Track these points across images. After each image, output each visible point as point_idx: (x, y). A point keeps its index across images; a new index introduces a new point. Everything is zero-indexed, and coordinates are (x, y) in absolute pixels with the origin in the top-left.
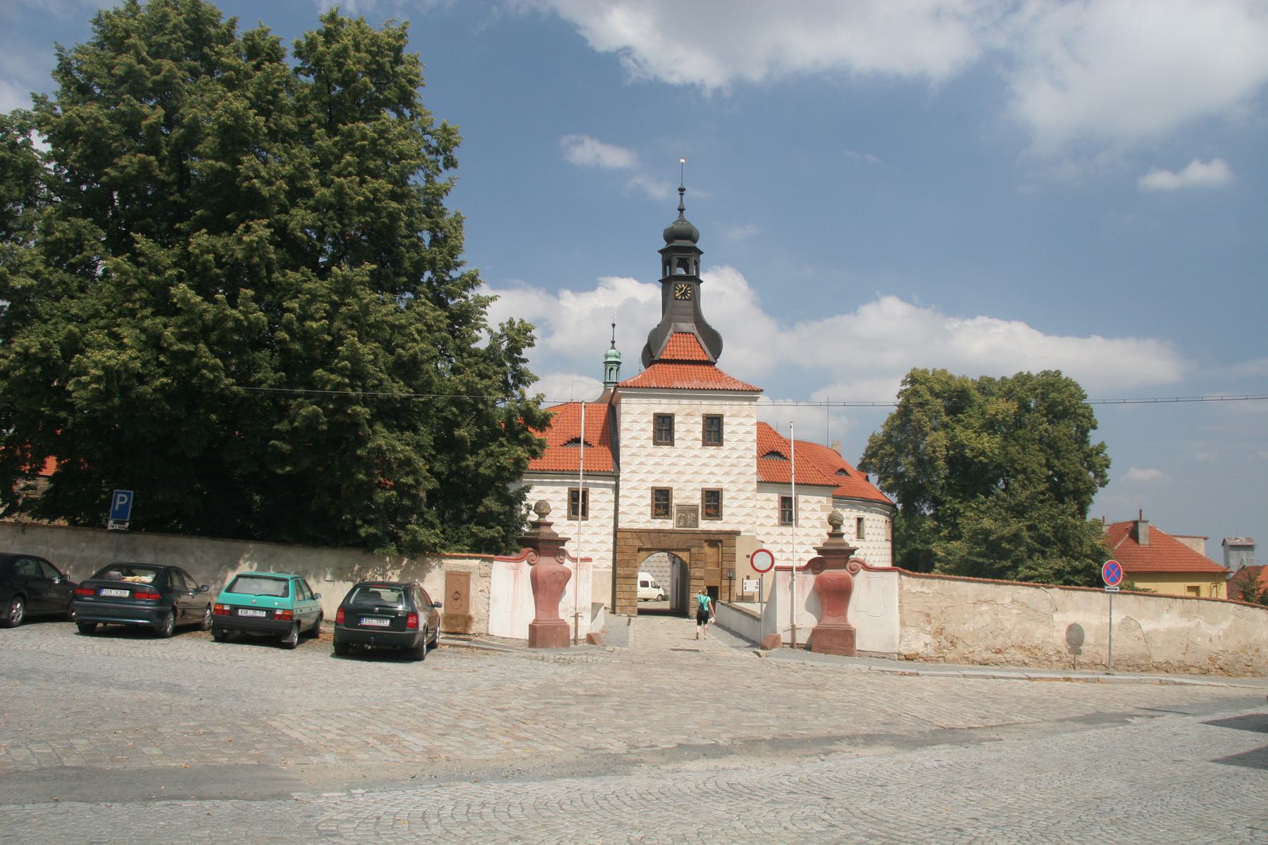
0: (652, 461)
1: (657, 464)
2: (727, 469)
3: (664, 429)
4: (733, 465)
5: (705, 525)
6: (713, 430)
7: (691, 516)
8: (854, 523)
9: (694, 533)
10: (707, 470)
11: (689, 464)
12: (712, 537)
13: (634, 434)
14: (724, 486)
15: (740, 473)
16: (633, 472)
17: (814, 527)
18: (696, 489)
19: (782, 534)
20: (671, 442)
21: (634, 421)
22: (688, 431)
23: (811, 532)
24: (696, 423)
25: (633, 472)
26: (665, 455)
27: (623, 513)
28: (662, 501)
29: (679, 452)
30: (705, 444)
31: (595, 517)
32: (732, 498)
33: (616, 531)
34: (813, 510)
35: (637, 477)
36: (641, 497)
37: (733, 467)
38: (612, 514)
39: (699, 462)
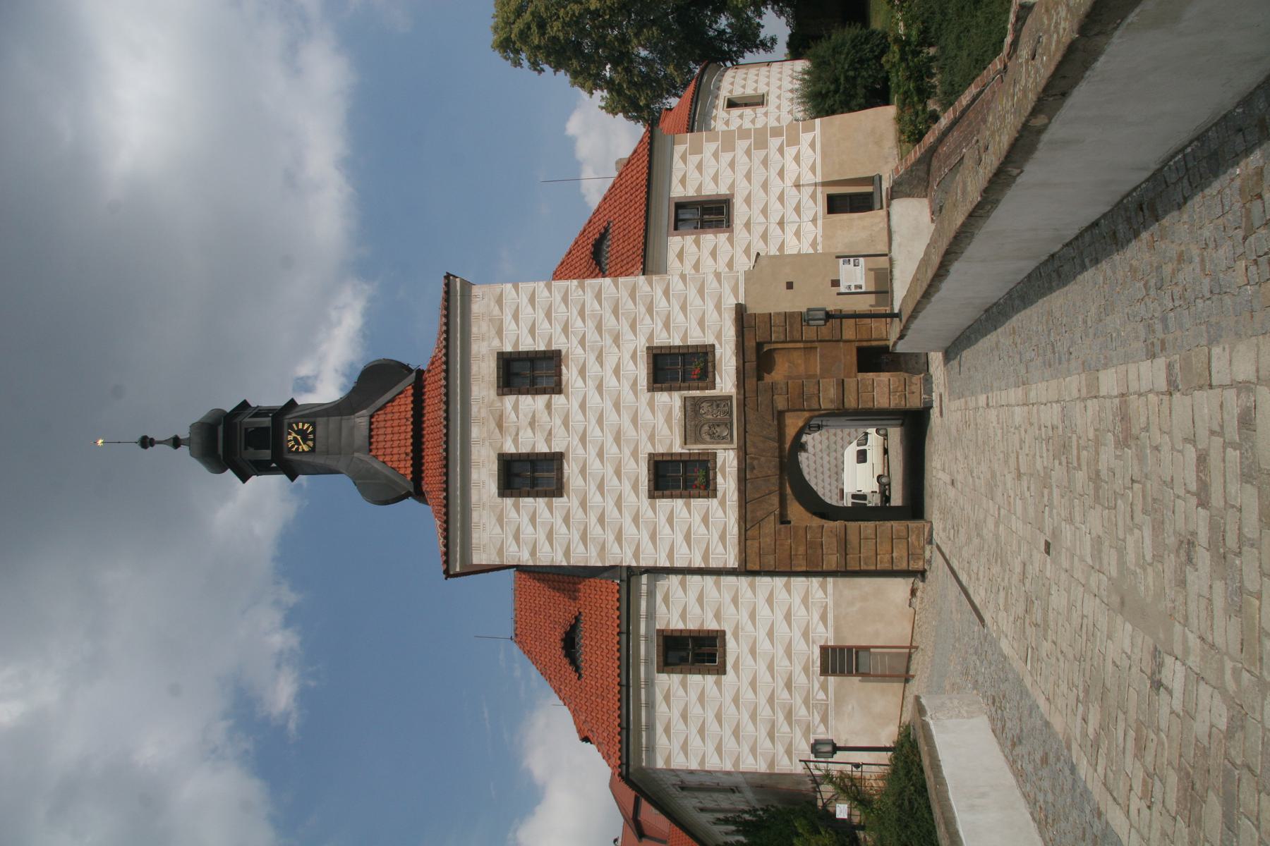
0: (595, 498)
1: (601, 487)
2: (608, 340)
3: (530, 475)
4: (599, 328)
5: (726, 383)
6: (529, 372)
7: (708, 413)
8: (736, 112)
9: (743, 404)
10: (610, 381)
11: (600, 421)
12: (751, 365)
13: (542, 537)
14: (642, 343)
15: (616, 312)
16: (619, 538)
17: (732, 165)
18: (651, 405)
19: (748, 225)
20: (555, 460)
21: (517, 537)
22: (532, 424)
23: (741, 169)
24: (516, 408)
25: (619, 538)
26: (583, 471)
27: (706, 557)
28: (674, 477)
29: (576, 441)
30: (557, 389)
31: (718, 616)
32: (667, 326)
33: (743, 570)
34: (699, 167)
35: (629, 529)
36: (670, 520)
37: (604, 331)
38: (709, 580)
39: (594, 399)
